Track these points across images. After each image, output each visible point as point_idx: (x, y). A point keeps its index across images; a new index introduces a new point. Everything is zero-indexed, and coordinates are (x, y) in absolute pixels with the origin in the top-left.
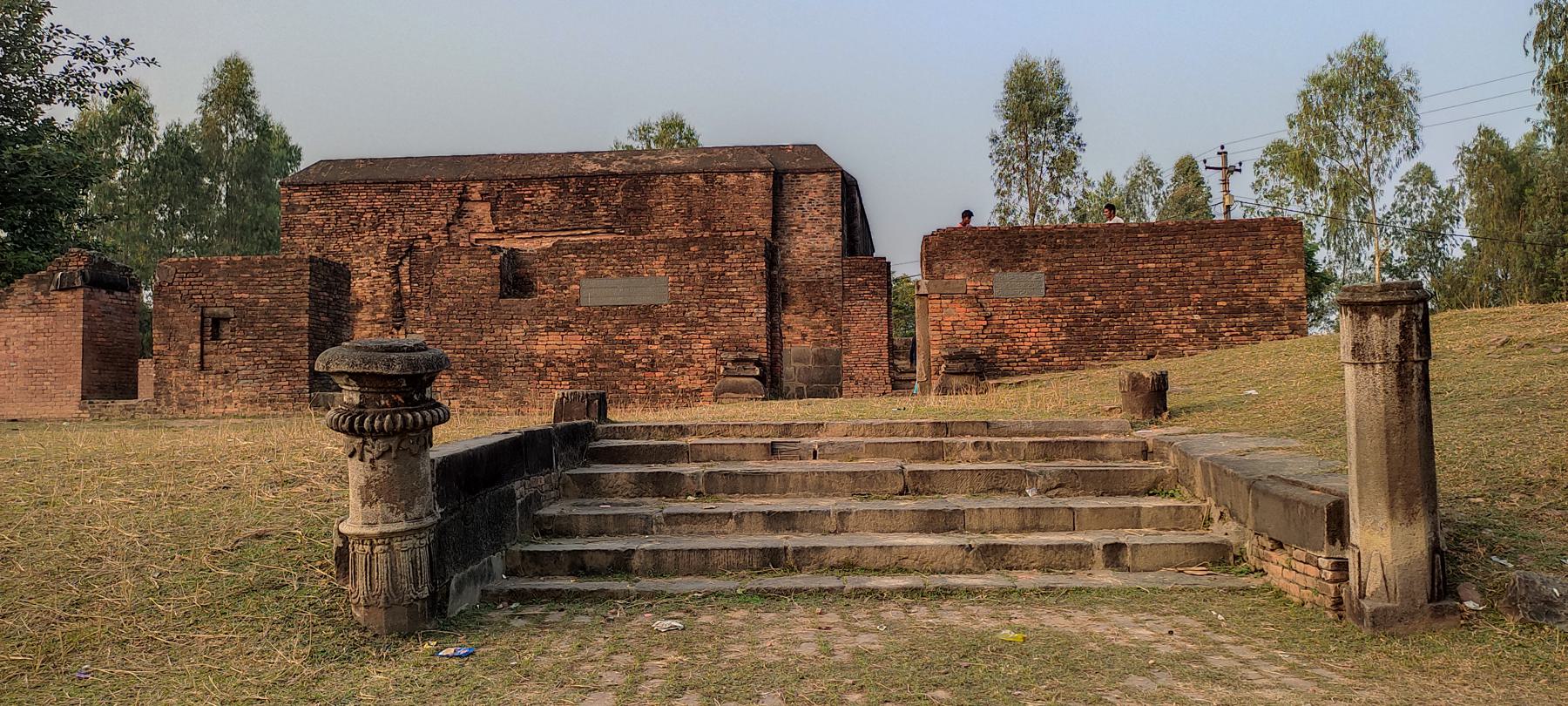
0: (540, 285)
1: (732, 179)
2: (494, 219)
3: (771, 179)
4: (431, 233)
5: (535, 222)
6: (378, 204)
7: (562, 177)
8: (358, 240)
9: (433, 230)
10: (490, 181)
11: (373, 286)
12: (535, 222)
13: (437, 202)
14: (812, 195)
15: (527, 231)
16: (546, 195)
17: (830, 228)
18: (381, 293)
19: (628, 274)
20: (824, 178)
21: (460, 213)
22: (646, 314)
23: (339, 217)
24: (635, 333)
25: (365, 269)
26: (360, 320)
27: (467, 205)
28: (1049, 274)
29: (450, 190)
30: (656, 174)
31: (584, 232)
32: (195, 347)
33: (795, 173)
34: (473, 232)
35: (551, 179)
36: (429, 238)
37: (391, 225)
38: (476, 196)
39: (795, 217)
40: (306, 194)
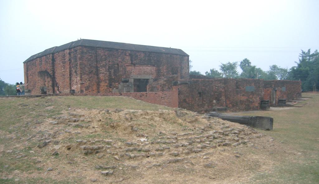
1: (175, 56)
2: (132, 60)
4: (119, 63)
6: (106, 54)
7: (145, 52)
8: (101, 63)
9: (119, 62)
11: (104, 76)
13: (120, 55)
15: (139, 64)
18: (107, 78)
25: (103, 71)
26: (101, 85)
29: (123, 52)
31: (149, 65)
34: (126, 63)
35: (143, 52)
36: (118, 64)
37: (109, 60)
38: (128, 54)
40: (87, 49)
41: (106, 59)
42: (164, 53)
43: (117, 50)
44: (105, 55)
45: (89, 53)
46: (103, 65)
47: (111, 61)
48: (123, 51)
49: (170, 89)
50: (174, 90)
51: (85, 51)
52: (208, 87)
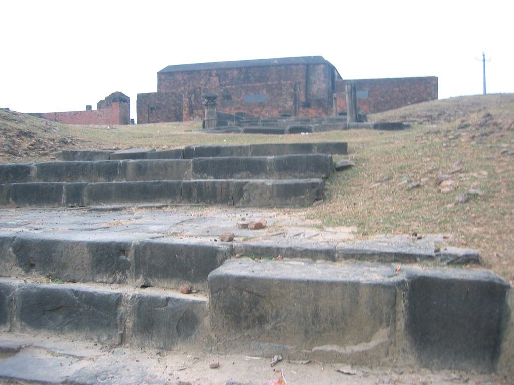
0: (233, 97)
1: (294, 67)
2: (220, 82)
3: (305, 67)
5: (232, 82)
6: (185, 78)
10: (218, 69)
12: (232, 82)
14: (319, 71)
16: (236, 72)
17: (324, 82)
19: (256, 94)
20: (323, 66)
21: (209, 80)
22: (261, 105)
23: (174, 82)
24: (258, 109)
27: (211, 78)
28: (369, 92)
29: (206, 73)
30: (269, 66)
32: (147, 116)
33: (314, 65)
35: (237, 69)
36: (200, 88)
38: (214, 74)
39: (312, 78)
41: (185, 84)
42: (273, 66)
43: (199, 72)
44: (184, 80)
45: (168, 79)
46: (182, 90)
47: (191, 85)
48: (206, 72)
49: (109, 105)
50: (114, 106)
51: (163, 78)
52: (165, 101)
